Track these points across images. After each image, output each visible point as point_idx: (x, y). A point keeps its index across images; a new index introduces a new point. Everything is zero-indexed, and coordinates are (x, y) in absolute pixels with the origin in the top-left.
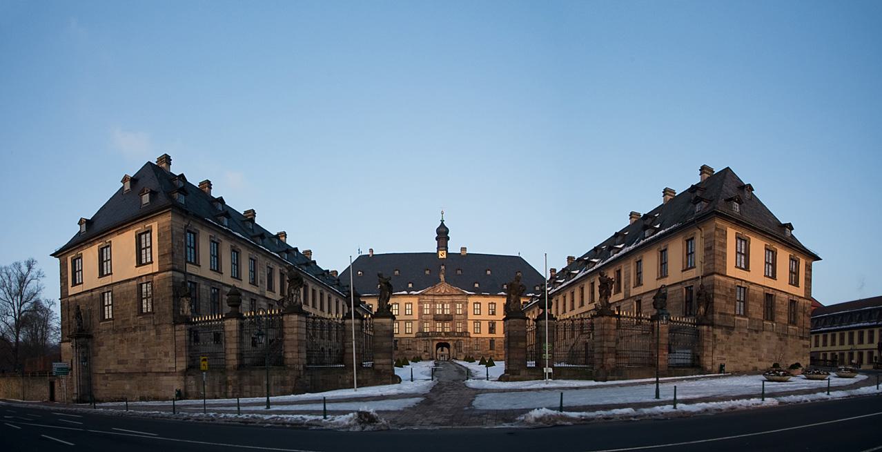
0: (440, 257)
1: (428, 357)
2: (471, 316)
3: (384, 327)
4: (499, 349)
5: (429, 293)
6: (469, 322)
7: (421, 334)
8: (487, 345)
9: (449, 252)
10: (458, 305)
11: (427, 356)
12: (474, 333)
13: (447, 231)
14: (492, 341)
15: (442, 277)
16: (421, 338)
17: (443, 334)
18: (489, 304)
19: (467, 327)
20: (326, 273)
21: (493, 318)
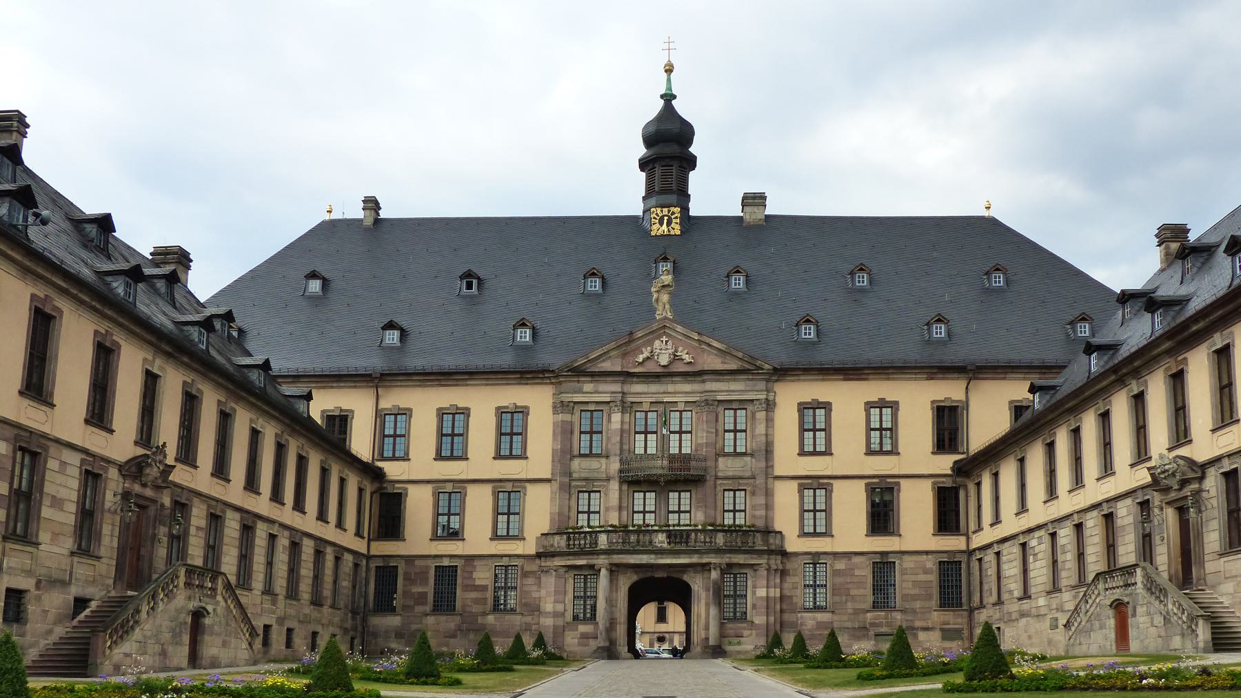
1: (593, 644)
4: (918, 605)
5: (606, 366)
7: (560, 542)
8: (860, 584)
11: (584, 636)
12: (803, 534)
14: (883, 566)
16: (558, 562)
17: (661, 540)
18: (869, 406)
19: (769, 507)
20: (92, 230)
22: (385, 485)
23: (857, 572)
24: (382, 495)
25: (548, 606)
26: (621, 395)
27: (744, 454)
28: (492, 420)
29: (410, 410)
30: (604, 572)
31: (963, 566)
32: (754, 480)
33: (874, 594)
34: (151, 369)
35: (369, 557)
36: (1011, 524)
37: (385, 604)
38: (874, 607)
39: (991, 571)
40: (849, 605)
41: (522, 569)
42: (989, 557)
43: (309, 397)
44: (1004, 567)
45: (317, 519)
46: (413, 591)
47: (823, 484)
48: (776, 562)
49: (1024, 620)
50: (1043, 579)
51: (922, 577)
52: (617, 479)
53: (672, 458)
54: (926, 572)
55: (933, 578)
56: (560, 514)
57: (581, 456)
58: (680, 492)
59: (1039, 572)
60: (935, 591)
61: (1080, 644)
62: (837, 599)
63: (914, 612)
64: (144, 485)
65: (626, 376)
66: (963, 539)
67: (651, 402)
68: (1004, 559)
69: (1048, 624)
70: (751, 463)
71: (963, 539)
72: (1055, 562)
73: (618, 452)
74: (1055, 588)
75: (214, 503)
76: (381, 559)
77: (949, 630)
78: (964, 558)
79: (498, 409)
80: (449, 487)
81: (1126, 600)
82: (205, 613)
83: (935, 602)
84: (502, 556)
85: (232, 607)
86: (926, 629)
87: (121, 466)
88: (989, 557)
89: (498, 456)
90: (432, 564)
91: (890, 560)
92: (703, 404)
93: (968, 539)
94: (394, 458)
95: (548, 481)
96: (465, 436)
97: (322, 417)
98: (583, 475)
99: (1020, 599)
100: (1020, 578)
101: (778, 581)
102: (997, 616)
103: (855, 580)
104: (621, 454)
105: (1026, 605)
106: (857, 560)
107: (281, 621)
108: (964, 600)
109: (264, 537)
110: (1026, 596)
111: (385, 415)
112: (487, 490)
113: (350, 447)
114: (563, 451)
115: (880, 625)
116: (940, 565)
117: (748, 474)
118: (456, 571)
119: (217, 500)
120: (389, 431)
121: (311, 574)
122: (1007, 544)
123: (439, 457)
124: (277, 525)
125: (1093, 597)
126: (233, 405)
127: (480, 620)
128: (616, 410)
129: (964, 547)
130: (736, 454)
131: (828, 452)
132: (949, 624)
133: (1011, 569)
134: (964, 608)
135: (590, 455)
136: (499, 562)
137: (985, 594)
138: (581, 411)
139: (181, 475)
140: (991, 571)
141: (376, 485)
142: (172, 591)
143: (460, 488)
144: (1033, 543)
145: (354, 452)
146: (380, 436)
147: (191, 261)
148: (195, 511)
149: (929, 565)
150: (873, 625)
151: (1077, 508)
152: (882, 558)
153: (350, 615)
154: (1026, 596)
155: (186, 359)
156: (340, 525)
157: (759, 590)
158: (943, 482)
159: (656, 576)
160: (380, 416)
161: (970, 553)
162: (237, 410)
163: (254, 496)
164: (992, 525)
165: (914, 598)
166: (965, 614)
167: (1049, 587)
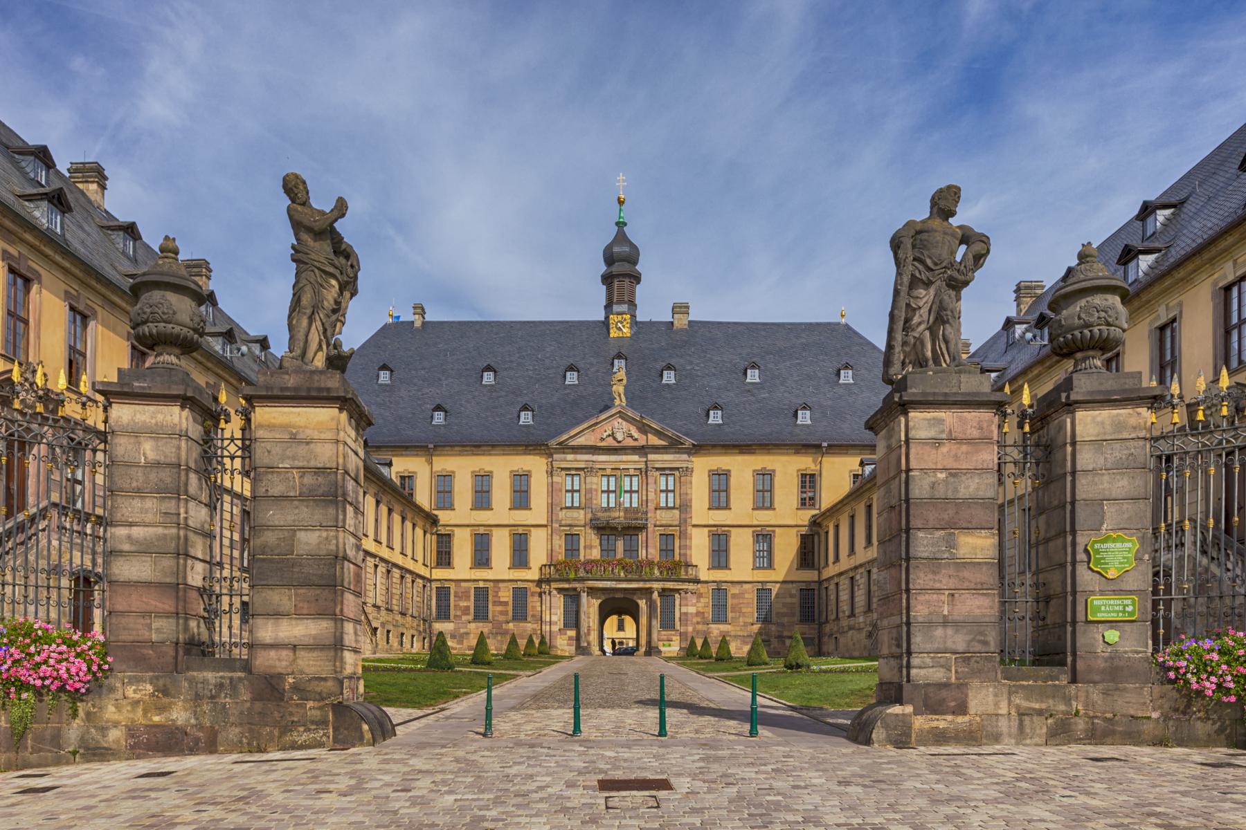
3: (302, 450)
4: (785, 620)
6: (695, 532)
36: (845, 563)
39: (833, 597)
42: (832, 587)
44: (841, 594)
50: (862, 603)
53: (626, 510)
60: (797, 610)
66: (816, 572)
68: (841, 588)
71: (816, 572)
72: (869, 591)
74: (869, 609)
78: (815, 586)
84: (517, 581)
88: (832, 587)
90: (472, 585)
95: (546, 526)
98: (569, 522)
99: (849, 617)
100: (849, 602)
102: (835, 629)
103: (745, 601)
105: (852, 621)
106: (746, 586)
107: (383, 625)
110: (852, 615)
112: (506, 532)
122: (843, 577)
129: (816, 578)
130: (667, 508)
133: (844, 596)
135: (572, 508)
137: (829, 613)
140: (833, 597)
144: (858, 577)
149: (794, 592)
154: (852, 615)
161: (820, 582)
164: (834, 563)
167: (866, 609)
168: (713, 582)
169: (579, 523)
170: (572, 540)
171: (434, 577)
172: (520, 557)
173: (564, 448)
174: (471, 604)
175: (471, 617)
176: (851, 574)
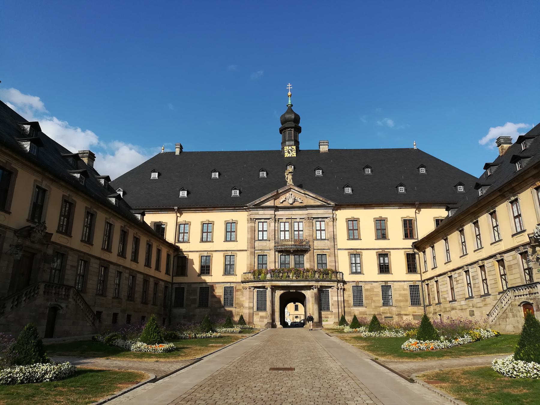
0: (287, 155)
2: (343, 241)
4: (402, 304)
8: (377, 295)
9: (301, 148)
10: (318, 223)
11: (262, 317)
13: (297, 119)
15: (289, 178)
21: (382, 244)
22: (179, 253)
23: (375, 290)
24: (178, 257)
25: (246, 304)
26: (274, 215)
27: (325, 239)
28: (223, 227)
29: (190, 222)
30: (269, 289)
31: (420, 287)
32: (330, 250)
33: (383, 300)
34: (40, 185)
35: (172, 283)
37: (180, 303)
38: (383, 305)
40: (373, 304)
41: (236, 288)
43: (143, 215)
45: (145, 266)
46: (191, 298)
47: (358, 252)
48: (340, 285)
49: (454, 312)
51: (403, 292)
52: (274, 250)
54: (404, 290)
55: (408, 292)
56: (250, 265)
57: (259, 240)
58: (299, 255)
59: (462, 289)
61: (499, 325)
62: (367, 301)
63: (401, 307)
64: (33, 242)
65: (276, 208)
67: (286, 219)
69: (468, 313)
70: (328, 243)
73: (274, 239)
75: (83, 255)
76: (177, 284)
77: (416, 315)
79: (225, 221)
80: (205, 254)
81: (531, 302)
82: (60, 308)
83: (409, 302)
85: (80, 304)
86: (406, 315)
87: (15, 231)
89: (226, 241)
91: (390, 285)
92: (307, 219)
93: (421, 275)
94: (183, 242)
96: (212, 232)
97: (154, 225)
101: (342, 293)
103: (375, 293)
104: (275, 239)
105: (455, 304)
108: (422, 302)
109: (114, 272)
111: (180, 224)
112: (221, 254)
113: (166, 238)
114: (251, 238)
115: (386, 313)
116: (410, 287)
117: (327, 248)
118: (208, 289)
119: (85, 253)
120: (182, 231)
121: (142, 290)
123: (202, 241)
124: (121, 267)
125: (506, 300)
126: (95, 210)
127: (218, 310)
128: (272, 222)
131: (359, 239)
132: (416, 313)
134: (422, 305)
136: (226, 285)
138: (259, 222)
139: (58, 238)
141: (176, 253)
142: (33, 296)
143: (210, 254)
145: (167, 240)
146: (178, 232)
147: (95, 157)
148: (70, 258)
150: (383, 313)
151: (481, 258)
152: (385, 284)
153: (163, 308)
155: (63, 183)
156: (158, 268)
157: (333, 297)
158: (409, 252)
159: (291, 291)
160: (178, 225)
162: (98, 212)
163: (108, 253)
165: (400, 301)
166: (423, 308)
168: (353, 282)
169: (266, 248)
170: (262, 257)
171: (174, 281)
172: (229, 269)
173: (258, 206)
174: (197, 297)
175: (197, 305)
176: (449, 274)
